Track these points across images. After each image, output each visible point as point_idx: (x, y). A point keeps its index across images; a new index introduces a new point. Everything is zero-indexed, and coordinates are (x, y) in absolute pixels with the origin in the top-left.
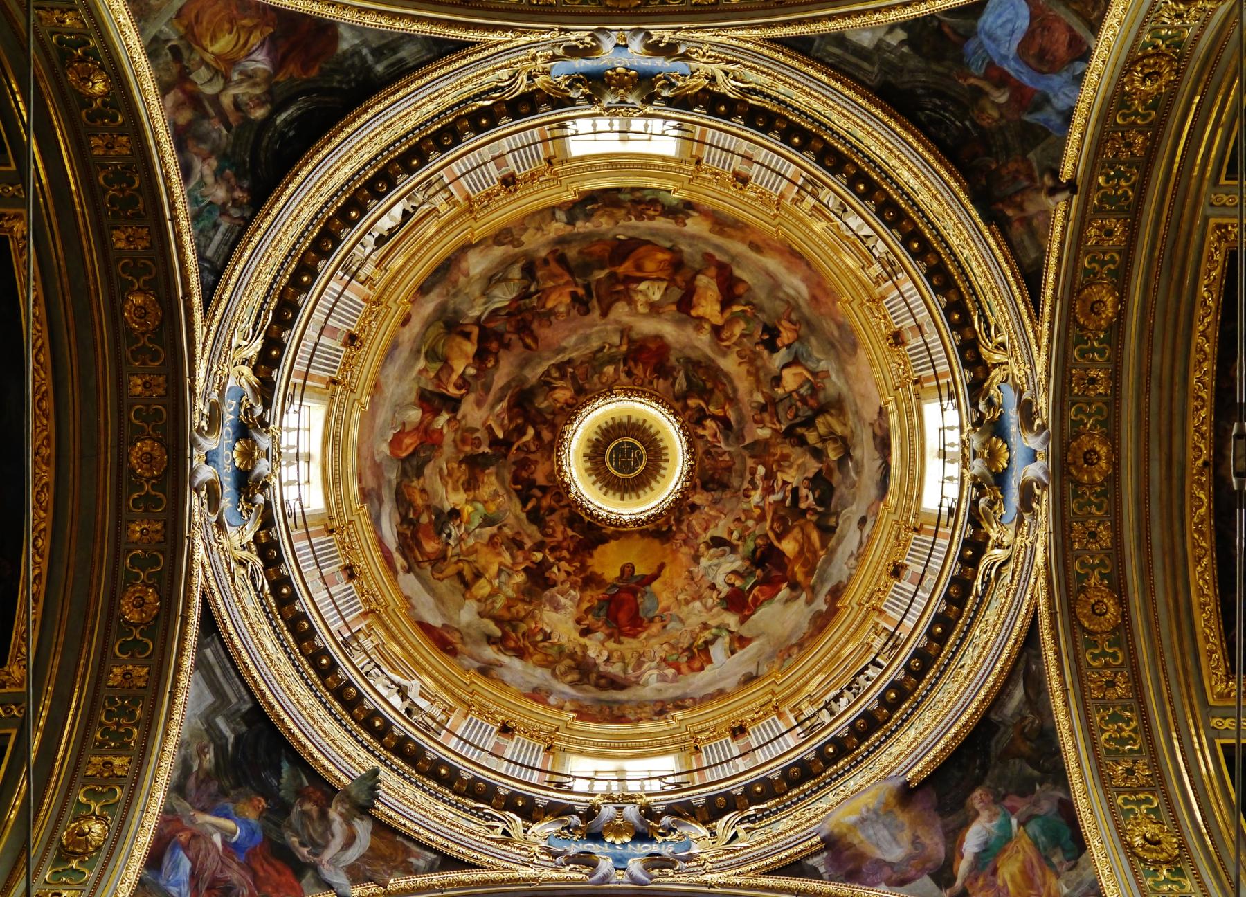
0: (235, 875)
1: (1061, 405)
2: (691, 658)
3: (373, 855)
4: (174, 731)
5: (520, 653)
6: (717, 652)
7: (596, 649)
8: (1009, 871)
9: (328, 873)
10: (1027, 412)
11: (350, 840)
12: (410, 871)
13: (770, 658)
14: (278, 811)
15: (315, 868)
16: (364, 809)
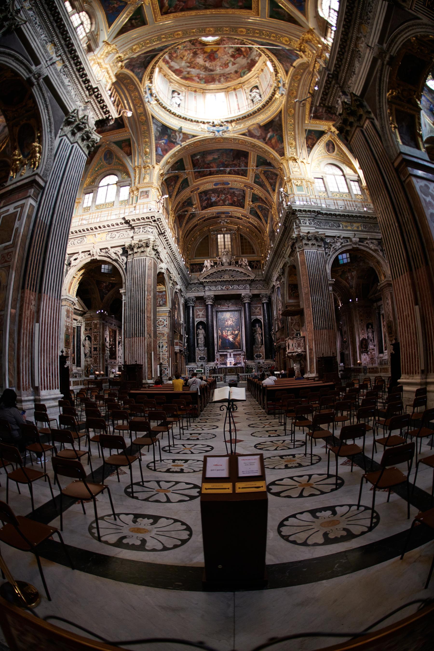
0: (166, 147)
1: (289, 87)
2: (225, 66)
3: (183, 138)
4: (153, 133)
5: (194, 68)
6: (230, 65)
7: (207, 64)
8: (273, 141)
9: (178, 142)
10: (284, 85)
11: (180, 137)
12: (189, 139)
13: (240, 68)
14: (169, 136)
15: (176, 142)
16: (181, 132)
